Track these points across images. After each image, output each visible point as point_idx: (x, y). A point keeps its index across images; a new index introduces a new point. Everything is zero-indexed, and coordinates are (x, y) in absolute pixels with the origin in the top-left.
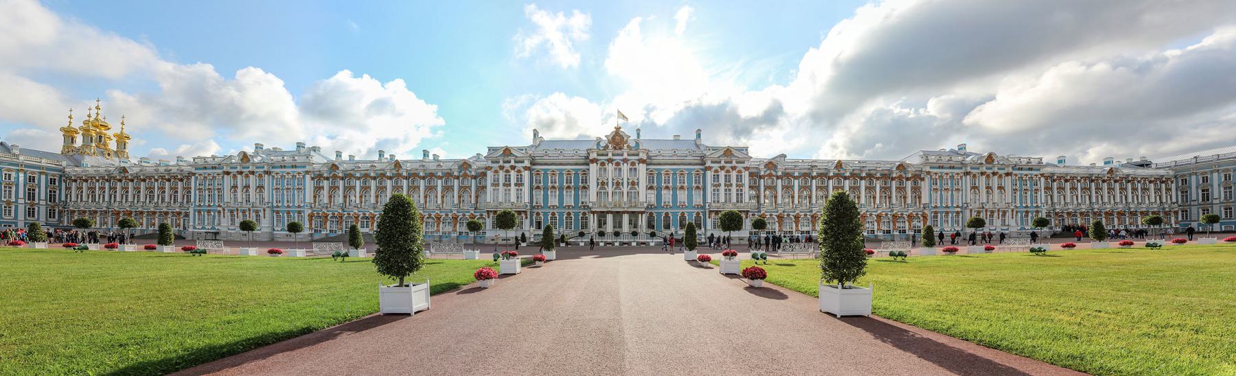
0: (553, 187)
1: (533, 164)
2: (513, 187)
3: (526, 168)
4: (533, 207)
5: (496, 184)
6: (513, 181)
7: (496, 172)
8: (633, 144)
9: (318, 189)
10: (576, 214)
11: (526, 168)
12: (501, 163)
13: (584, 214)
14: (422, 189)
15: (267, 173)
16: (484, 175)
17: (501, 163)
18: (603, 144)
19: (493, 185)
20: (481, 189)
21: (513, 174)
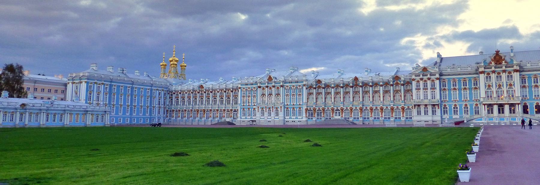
0: (455, 89)
1: (441, 75)
2: (429, 91)
3: (437, 79)
4: (442, 102)
5: (418, 89)
6: (429, 86)
7: (418, 81)
8: (509, 60)
9: (310, 94)
10: (471, 105)
11: (437, 79)
12: (421, 76)
13: (477, 105)
14: (361, 92)
15: (282, 86)
16: (411, 84)
17: (421, 76)
18: (488, 61)
19: (416, 89)
20: (408, 91)
21: (429, 82)
